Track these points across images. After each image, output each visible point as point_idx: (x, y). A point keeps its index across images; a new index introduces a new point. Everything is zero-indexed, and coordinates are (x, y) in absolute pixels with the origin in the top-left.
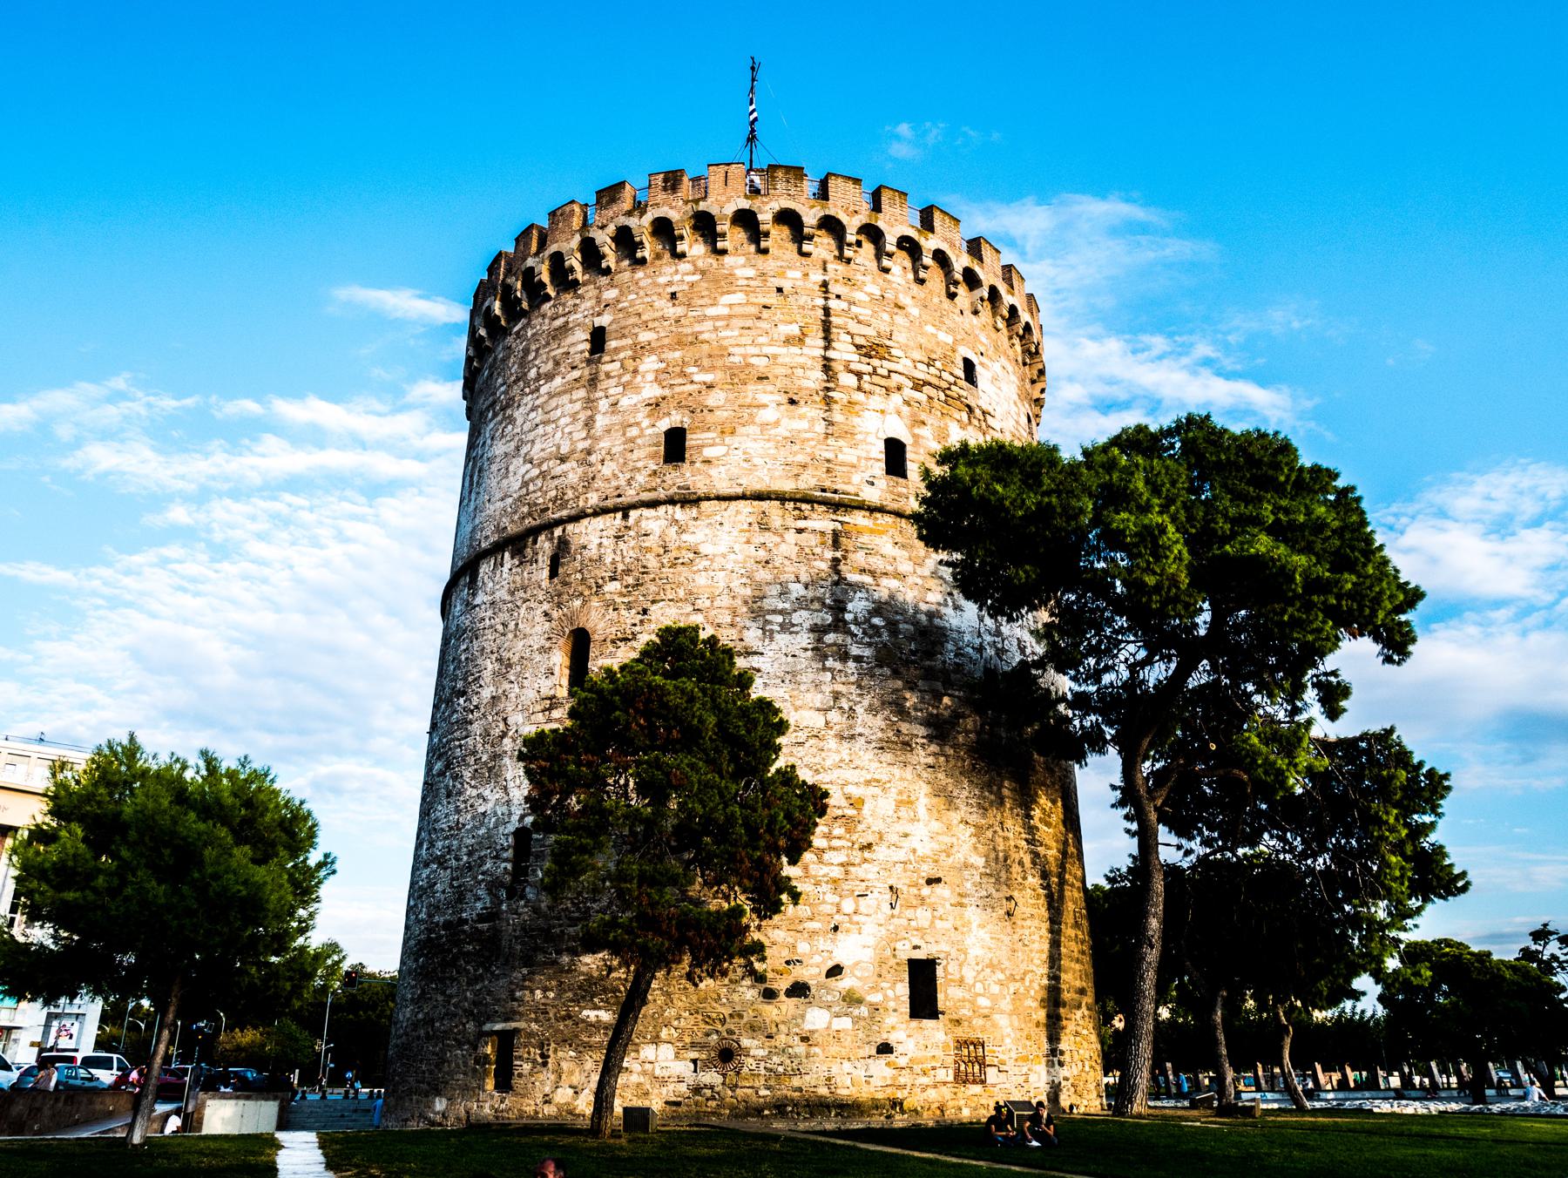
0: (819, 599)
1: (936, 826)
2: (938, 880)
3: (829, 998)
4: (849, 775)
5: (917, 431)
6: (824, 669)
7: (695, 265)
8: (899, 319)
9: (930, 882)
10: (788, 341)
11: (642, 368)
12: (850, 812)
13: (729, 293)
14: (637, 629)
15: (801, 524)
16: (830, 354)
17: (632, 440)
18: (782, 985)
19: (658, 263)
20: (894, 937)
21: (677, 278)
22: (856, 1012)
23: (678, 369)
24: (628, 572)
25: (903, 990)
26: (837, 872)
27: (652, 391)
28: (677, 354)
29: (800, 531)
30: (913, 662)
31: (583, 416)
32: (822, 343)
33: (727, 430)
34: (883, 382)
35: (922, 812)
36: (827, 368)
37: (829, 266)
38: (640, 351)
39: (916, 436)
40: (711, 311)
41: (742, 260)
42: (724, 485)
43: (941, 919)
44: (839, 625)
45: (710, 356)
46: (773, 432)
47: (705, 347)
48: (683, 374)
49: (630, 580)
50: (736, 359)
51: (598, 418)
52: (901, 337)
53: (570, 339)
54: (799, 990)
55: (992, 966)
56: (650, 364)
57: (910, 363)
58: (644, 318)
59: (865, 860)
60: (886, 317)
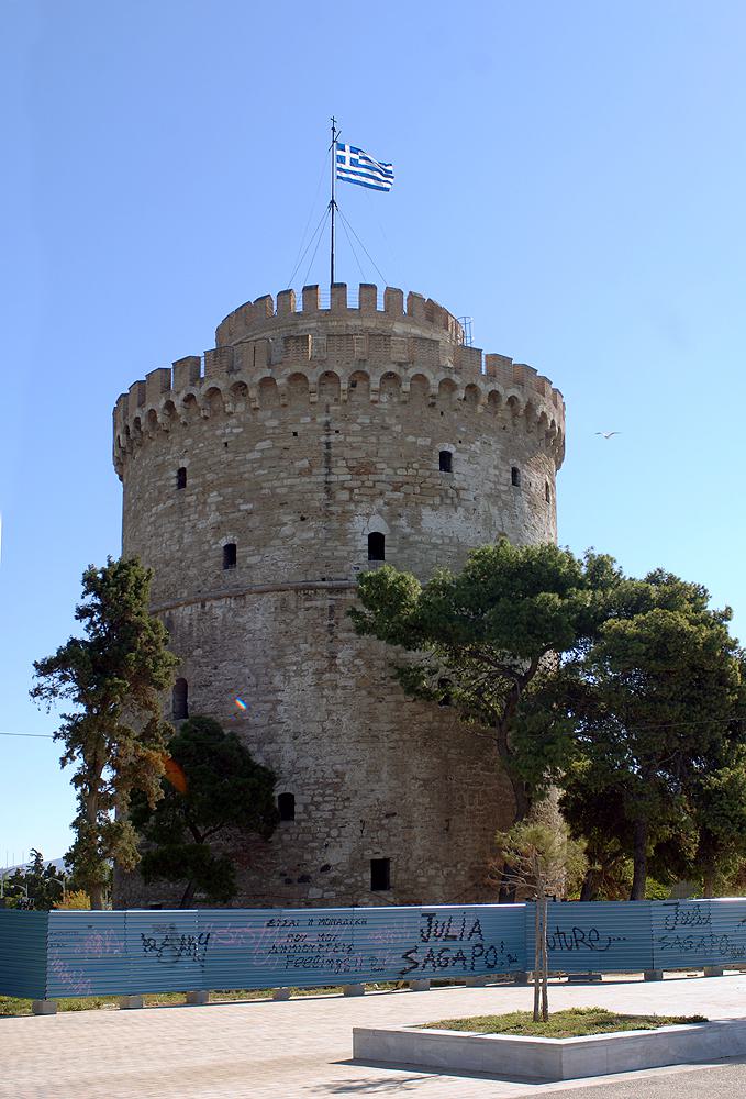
0: (319, 653)
1: (393, 783)
2: (395, 814)
3: (322, 882)
4: (337, 759)
5: (394, 523)
6: (322, 697)
7: (239, 420)
8: (384, 439)
9: (387, 816)
10: (301, 473)
11: (209, 501)
12: (336, 781)
13: (262, 440)
14: (213, 679)
15: (308, 604)
16: (332, 478)
17: (205, 553)
18: (296, 877)
19: (216, 418)
20: (362, 849)
21: (228, 430)
22: (338, 889)
23: (229, 501)
24: (206, 642)
25: (368, 876)
26: (327, 815)
27: (214, 517)
28: (230, 490)
29: (307, 609)
30: (382, 685)
31: (176, 534)
32: (324, 471)
33: (262, 544)
34: (368, 492)
35: (384, 775)
36: (328, 491)
37: (331, 408)
38: (207, 488)
39: (393, 529)
40: (250, 456)
41: (269, 413)
42: (260, 582)
43: (394, 836)
44: (332, 667)
45: (250, 491)
46: (290, 543)
47: (247, 483)
48: (234, 505)
49: (207, 648)
50: (266, 491)
51: (185, 536)
52: (384, 453)
53: (167, 475)
54: (305, 879)
55: (431, 860)
56: (214, 497)
57: (390, 471)
58: (209, 462)
59: (345, 807)
60: (374, 439)
